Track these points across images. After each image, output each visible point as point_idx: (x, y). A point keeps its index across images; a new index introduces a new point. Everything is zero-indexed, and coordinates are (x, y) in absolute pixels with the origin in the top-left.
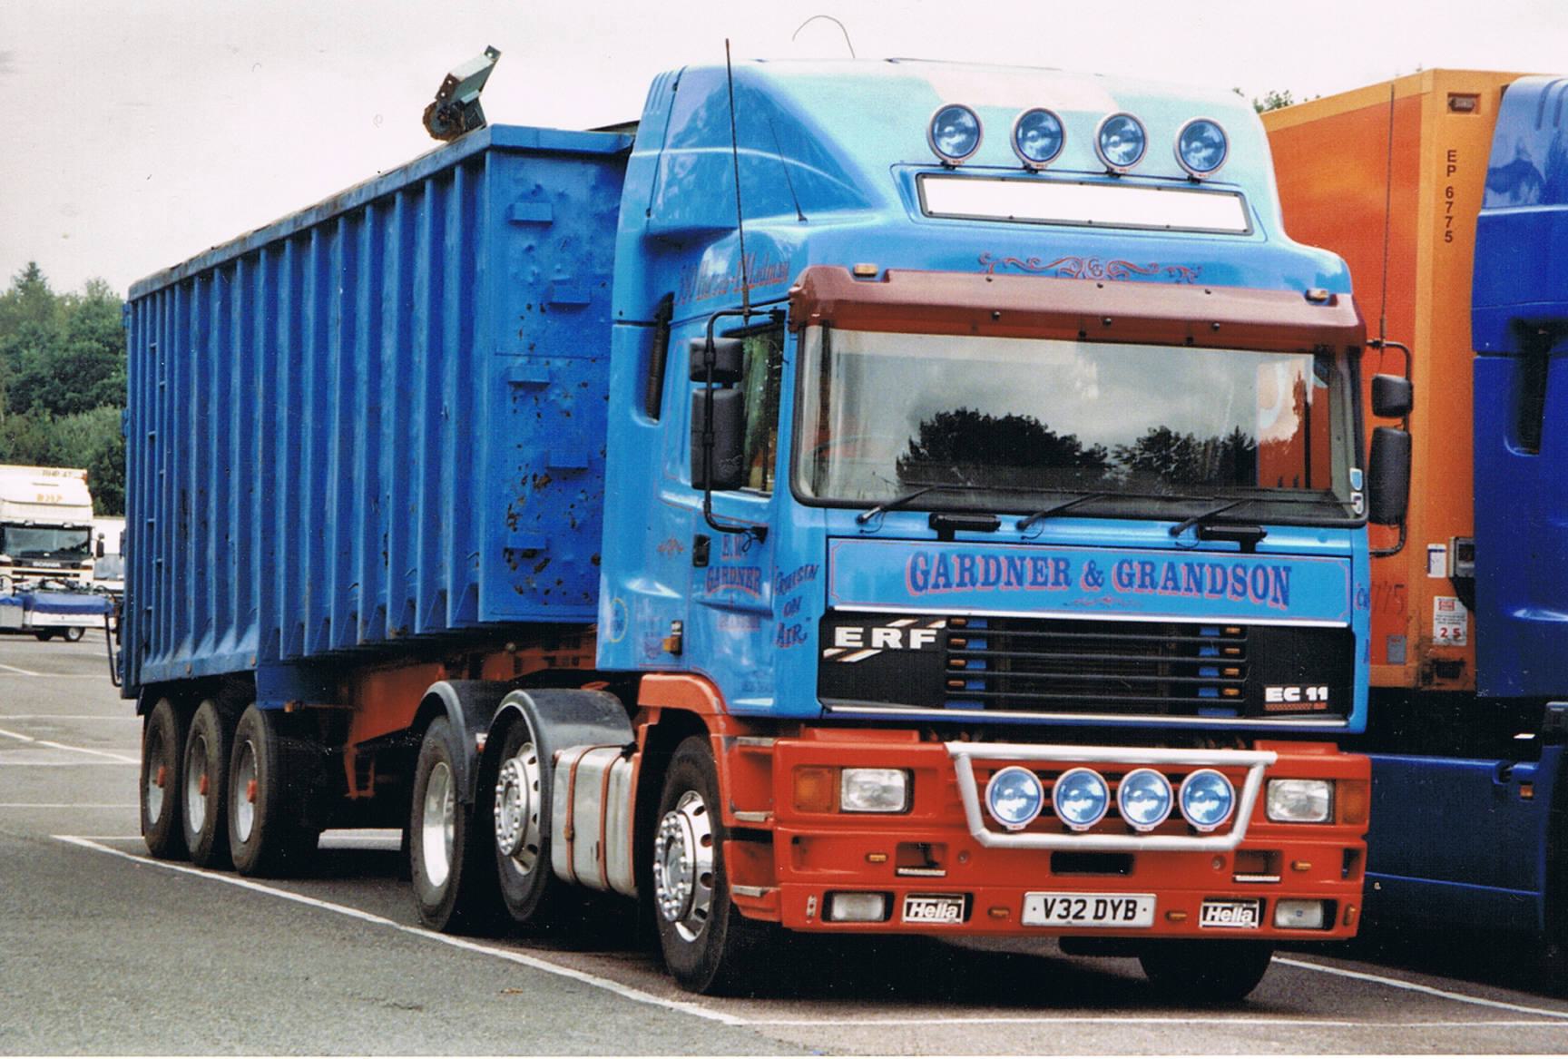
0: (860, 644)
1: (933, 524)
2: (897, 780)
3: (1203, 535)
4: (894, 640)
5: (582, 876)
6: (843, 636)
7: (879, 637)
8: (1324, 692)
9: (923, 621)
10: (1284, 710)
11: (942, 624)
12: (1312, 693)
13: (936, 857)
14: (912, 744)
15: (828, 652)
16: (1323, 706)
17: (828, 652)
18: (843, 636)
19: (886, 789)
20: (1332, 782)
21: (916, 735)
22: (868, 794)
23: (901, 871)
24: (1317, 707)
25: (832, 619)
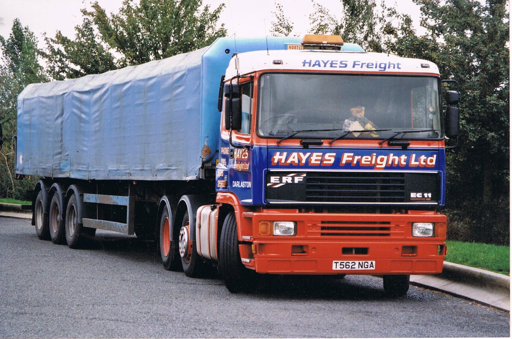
1: (302, 144)
2: (291, 225)
3: (390, 145)
4: (290, 181)
5: (202, 252)
6: (273, 179)
7: (285, 179)
8: (430, 195)
9: (299, 174)
10: (417, 200)
11: (305, 175)
12: (426, 195)
13: (305, 250)
14: (297, 214)
15: (268, 185)
16: (429, 199)
17: (268, 185)
18: (273, 179)
19: (289, 229)
20: (434, 224)
21: (297, 211)
22: (282, 230)
23: (293, 254)
24: (427, 199)
25: (270, 174)
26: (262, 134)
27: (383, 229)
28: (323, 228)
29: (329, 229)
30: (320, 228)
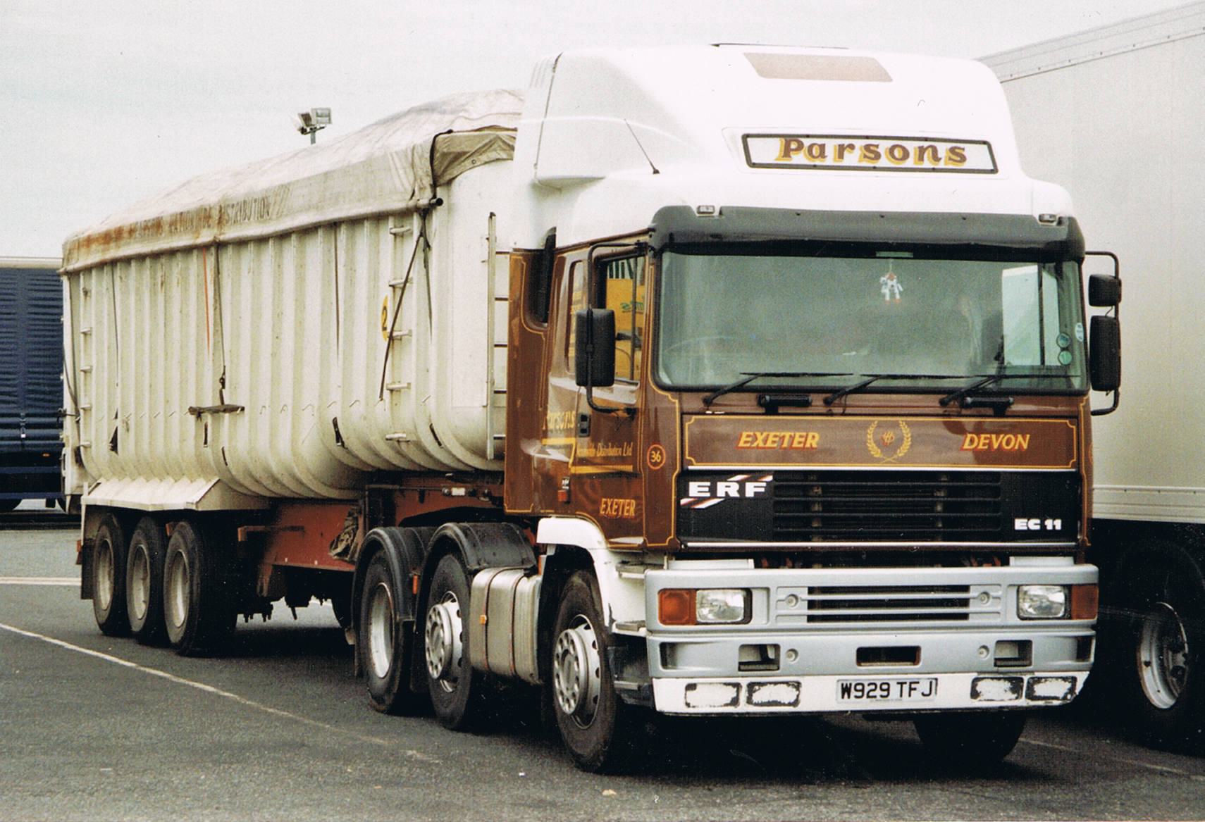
0: (708, 495)
4: (734, 492)
6: (696, 489)
7: (722, 488)
8: (1058, 524)
9: (755, 475)
10: (1028, 535)
11: (770, 478)
12: (1049, 524)
15: (683, 501)
17: (683, 501)
18: (696, 489)
21: (751, 561)
22: (716, 609)
25: (687, 476)
26: (666, 380)
27: (950, 607)
28: (811, 605)
29: (826, 608)
30: (806, 603)
